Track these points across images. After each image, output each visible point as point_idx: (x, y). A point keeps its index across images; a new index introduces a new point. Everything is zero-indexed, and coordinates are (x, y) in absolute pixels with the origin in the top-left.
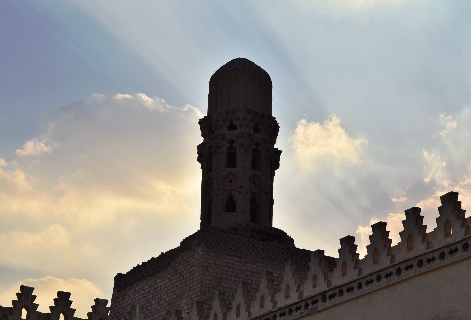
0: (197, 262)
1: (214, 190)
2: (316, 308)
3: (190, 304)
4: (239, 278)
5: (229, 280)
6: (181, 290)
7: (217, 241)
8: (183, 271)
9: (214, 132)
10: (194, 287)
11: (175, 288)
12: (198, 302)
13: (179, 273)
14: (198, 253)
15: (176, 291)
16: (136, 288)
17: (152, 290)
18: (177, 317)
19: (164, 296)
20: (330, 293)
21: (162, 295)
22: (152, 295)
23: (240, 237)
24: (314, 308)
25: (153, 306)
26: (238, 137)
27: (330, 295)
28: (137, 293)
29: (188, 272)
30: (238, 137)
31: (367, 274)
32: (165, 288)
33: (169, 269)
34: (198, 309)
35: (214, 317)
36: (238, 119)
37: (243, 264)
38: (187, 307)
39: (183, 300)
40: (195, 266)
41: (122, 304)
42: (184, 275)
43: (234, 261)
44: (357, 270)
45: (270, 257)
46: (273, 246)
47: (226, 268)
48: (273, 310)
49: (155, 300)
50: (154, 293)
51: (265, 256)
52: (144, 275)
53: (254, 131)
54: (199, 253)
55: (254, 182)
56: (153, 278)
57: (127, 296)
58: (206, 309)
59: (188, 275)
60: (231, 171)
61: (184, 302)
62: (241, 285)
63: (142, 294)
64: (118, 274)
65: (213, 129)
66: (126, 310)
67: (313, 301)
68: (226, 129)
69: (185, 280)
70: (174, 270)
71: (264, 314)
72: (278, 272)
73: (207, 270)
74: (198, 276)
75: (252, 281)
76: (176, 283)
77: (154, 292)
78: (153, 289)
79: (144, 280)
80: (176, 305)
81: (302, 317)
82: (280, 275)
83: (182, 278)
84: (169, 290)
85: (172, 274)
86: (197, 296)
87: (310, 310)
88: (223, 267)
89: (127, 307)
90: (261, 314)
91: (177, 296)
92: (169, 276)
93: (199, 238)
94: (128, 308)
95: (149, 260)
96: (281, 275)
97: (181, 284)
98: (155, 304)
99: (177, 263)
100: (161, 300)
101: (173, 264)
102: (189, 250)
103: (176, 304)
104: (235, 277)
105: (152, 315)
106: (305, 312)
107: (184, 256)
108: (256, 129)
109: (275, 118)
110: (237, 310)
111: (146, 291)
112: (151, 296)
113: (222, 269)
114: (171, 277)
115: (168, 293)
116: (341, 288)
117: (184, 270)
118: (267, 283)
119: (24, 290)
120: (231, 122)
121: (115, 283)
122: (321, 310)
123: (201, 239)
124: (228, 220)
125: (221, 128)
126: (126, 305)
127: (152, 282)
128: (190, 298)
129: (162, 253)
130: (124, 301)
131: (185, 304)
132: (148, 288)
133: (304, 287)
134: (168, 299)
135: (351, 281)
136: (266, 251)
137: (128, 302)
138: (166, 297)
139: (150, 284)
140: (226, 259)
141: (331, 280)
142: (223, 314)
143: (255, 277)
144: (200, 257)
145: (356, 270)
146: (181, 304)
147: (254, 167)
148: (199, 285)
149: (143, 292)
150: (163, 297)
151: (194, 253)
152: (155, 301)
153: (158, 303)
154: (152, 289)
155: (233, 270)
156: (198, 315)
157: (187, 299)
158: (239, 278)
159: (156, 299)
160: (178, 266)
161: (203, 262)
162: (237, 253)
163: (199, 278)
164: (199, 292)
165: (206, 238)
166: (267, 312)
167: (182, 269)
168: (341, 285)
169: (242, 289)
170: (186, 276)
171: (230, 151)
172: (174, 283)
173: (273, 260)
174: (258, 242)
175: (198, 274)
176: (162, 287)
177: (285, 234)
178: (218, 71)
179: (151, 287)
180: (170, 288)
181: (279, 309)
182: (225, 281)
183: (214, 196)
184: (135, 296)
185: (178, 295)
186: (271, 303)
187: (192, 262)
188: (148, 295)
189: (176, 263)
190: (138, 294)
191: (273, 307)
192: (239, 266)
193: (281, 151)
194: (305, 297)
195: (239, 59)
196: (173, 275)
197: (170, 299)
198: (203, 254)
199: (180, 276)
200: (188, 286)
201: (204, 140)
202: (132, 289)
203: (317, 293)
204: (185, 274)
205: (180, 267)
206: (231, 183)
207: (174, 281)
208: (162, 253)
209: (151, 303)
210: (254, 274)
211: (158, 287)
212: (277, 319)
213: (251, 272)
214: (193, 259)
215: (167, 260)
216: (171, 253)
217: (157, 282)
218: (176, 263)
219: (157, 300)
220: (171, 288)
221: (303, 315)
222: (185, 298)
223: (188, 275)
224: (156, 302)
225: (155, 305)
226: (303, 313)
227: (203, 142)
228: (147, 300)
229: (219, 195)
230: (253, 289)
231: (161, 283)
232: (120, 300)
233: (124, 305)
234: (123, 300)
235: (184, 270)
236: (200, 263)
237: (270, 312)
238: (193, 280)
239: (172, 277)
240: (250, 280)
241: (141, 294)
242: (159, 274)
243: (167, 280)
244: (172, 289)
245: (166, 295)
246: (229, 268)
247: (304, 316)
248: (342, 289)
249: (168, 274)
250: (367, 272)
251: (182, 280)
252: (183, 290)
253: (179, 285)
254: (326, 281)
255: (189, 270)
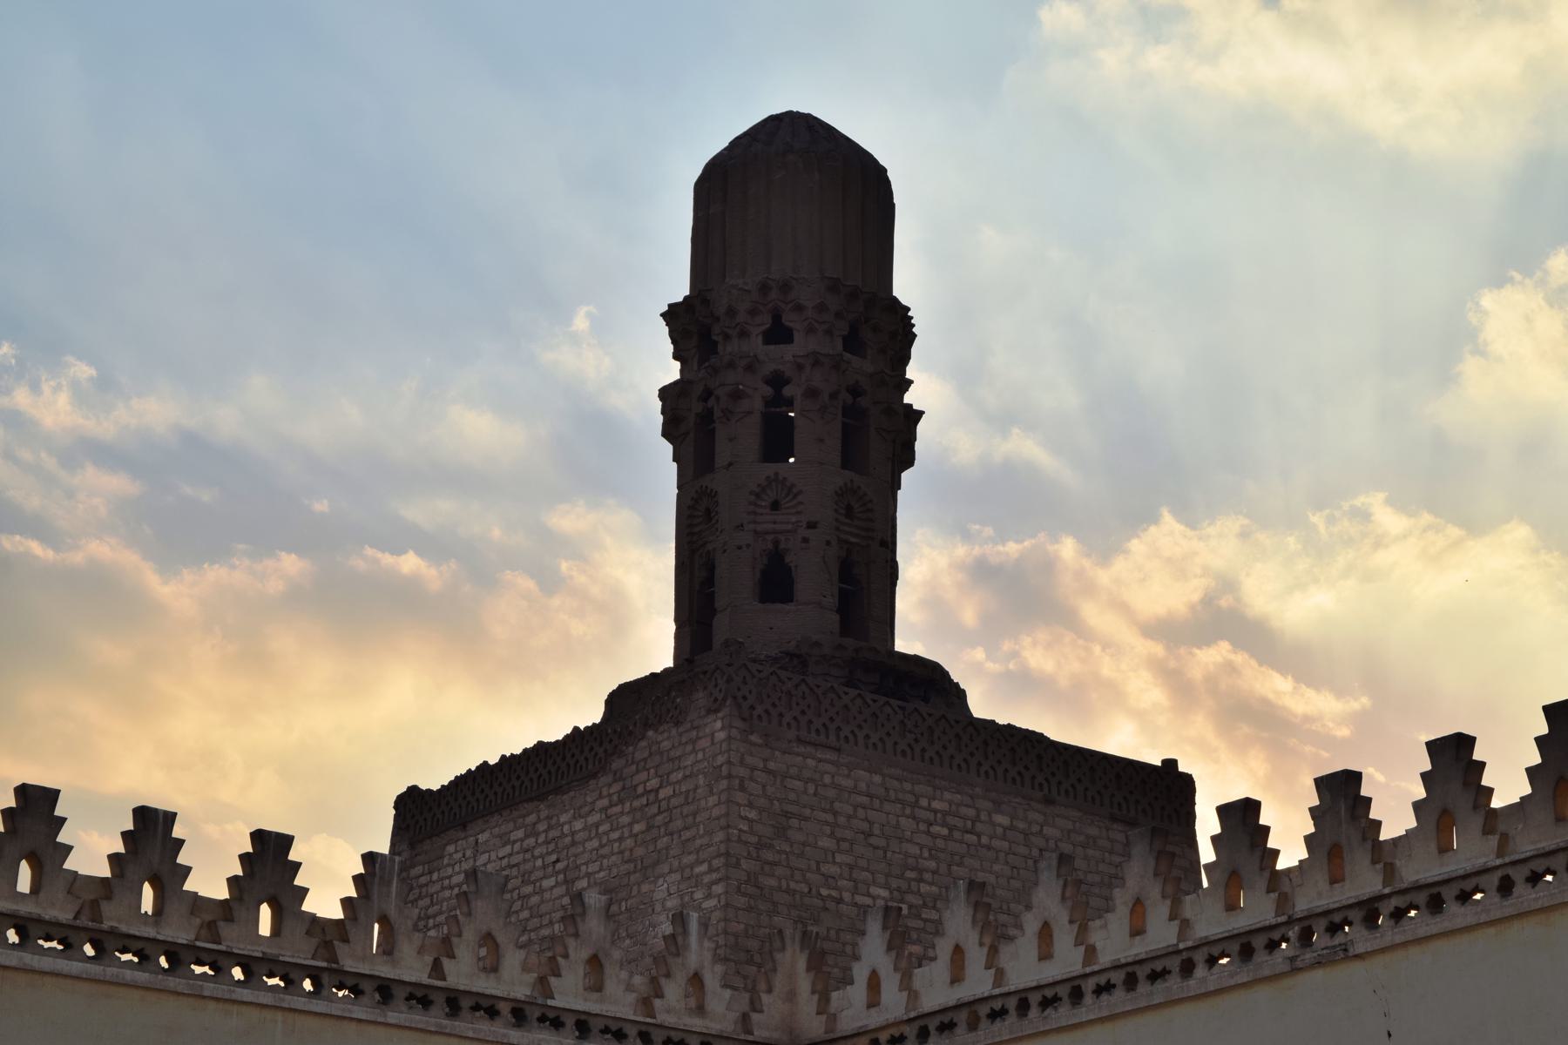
0: (708, 763)
1: (721, 532)
2: (1345, 944)
3: (686, 893)
4: (835, 814)
5: (806, 819)
6: (651, 848)
7: (769, 696)
8: (659, 788)
9: (720, 348)
10: (698, 842)
11: (629, 843)
12: (887, 909)
13: (642, 795)
14: (713, 734)
15: (631, 850)
16: (480, 836)
17: (540, 845)
18: (807, 952)
19: (586, 864)
20: (1395, 902)
21: (578, 863)
22: (543, 862)
23: (836, 686)
24: (1340, 945)
25: (547, 895)
26: (800, 367)
27: (1396, 908)
28: (484, 853)
29: (677, 792)
30: (800, 367)
31: (1531, 853)
32: (591, 839)
33: (602, 779)
34: (889, 932)
35: (952, 960)
36: (799, 308)
37: (846, 772)
38: (675, 901)
39: (661, 881)
40: (700, 776)
41: (426, 885)
42: (660, 801)
43: (820, 761)
44: (1493, 841)
45: (923, 750)
46: (930, 715)
47: (798, 783)
48: (1181, 946)
49: (552, 876)
50: (549, 854)
51: (909, 745)
52: (511, 796)
53: (846, 349)
54: (716, 734)
55: (849, 512)
56: (542, 806)
57: (446, 861)
58: (743, 909)
59: (674, 802)
60: (776, 474)
61: (666, 885)
62: (1054, 863)
63: (504, 855)
64: (409, 788)
65: (715, 338)
66: (445, 904)
67: (1331, 923)
68: (760, 338)
69: (665, 817)
70: (621, 783)
71: (1150, 956)
72: (947, 795)
73: (742, 788)
74: (716, 805)
75: (871, 823)
76: (631, 825)
77: (550, 850)
78: (547, 842)
79: (511, 811)
80: (633, 894)
81: (1295, 970)
82: (950, 805)
83: (654, 809)
84: (607, 848)
85: (615, 798)
86: (711, 870)
87: (1325, 952)
88: (788, 779)
89: (447, 893)
90: (1136, 955)
91: (635, 867)
92: (605, 802)
93: (716, 686)
94: (450, 898)
95: (525, 750)
96: (954, 807)
97: (649, 828)
98: (552, 888)
99: (633, 763)
100: (578, 878)
101: (617, 764)
102: (677, 724)
103: (635, 892)
104: (824, 810)
105: (546, 921)
106: (1304, 954)
107: (659, 743)
108: (853, 343)
109: (909, 309)
110: (1040, 937)
111: (517, 847)
112: (539, 863)
113: (785, 787)
114: (611, 806)
115: (604, 857)
116: (1434, 890)
117: (661, 784)
118: (1152, 863)
119: (377, 866)
120: (777, 318)
121: (396, 817)
122: (1367, 953)
123: (720, 691)
124: (771, 628)
125: (744, 334)
126: (443, 888)
127: (539, 820)
128: (686, 875)
129: (576, 729)
130: (435, 876)
131: (668, 891)
132: (527, 836)
133: (1290, 880)
134: (602, 874)
135: (1474, 870)
136: (910, 732)
137: (450, 877)
138: (593, 868)
139: (535, 824)
140: (798, 754)
141: (1398, 863)
142: (985, 950)
143: (881, 811)
144: (718, 746)
145: (1489, 837)
146: (653, 891)
147: (846, 463)
148: (720, 836)
149: (508, 849)
150: (583, 868)
151: (695, 733)
152: (553, 879)
153: (564, 887)
154: (539, 841)
155: (816, 789)
156: (890, 948)
157: (676, 877)
158: (835, 814)
159: (558, 873)
160: (638, 772)
161: (729, 762)
162: (827, 737)
163: (716, 812)
164: (719, 856)
165: (739, 689)
166: (1158, 949)
167: (654, 783)
168: (1436, 879)
169: (1058, 876)
170: (668, 805)
171: (773, 409)
172: (624, 827)
173: (931, 759)
174: (887, 702)
175: (712, 800)
176: (578, 837)
177: (944, 674)
178: (726, 152)
179: (537, 835)
180: (609, 841)
181: (1204, 941)
182: (794, 822)
183: (725, 551)
184: (475, 860)
185: (639, 862)
186: (1172, 923)
187: (689, 763)
188: (525, 861)
189: (627, 761)
190: (489, 856)
191: (1181, 936)
192: (833, 777)
193: (921, 413)
194: (1302, 911)
195: (790, 114)
196: (621, 801)
197: (612, 876)
198: (729, 738)
199: (647, 805)
200: (675, 836)
201: (682, 371)
202: (465, 838)
203: (1350, 902)
204: (664, 799)
205: (643, 776)
206: (773, 512)
207: (625, 820)
208: (576, 729)
209: (540, 886)
210: (877, 803)
211: (563, 835)
212: (1195, 971)
213: (871, 796)
214: (694, 751)
215: (593, 753)
216: (610, 731)
217: (558, 820)
218: (630, 762)
219: (561, 877)
220: (615, 840)
221: (1299, 964)
222: (669, 873)
223: (674, 802)
224: (557, 882)
225: (555, 891)
226: (1299, 959)
227: (678, 377)
228: (523, 876)
229: (740, 548)
230: (876, 848)
231: (573, 823)
232: (418, 870)
233: (437, 887)
234: (430, 873)
235: (661, 787)
236: (721, 766)
237: (1171, 949)
238: (695, 818)
239: (616, 805)
240: (866, 819)
241: (500, 856)
242: (565, 797)
243: (599, 815)
244: (616, 845)
245: (596, 861)
246: (807, 783)
247: (1301, 968)
248: (1439, 894)
249: (601, 797)
250: (1533, 847)
251: (655, 815)
252: (658, 848)
253: (643, 832)
254: (1379, 866)
255: (680, 786)
